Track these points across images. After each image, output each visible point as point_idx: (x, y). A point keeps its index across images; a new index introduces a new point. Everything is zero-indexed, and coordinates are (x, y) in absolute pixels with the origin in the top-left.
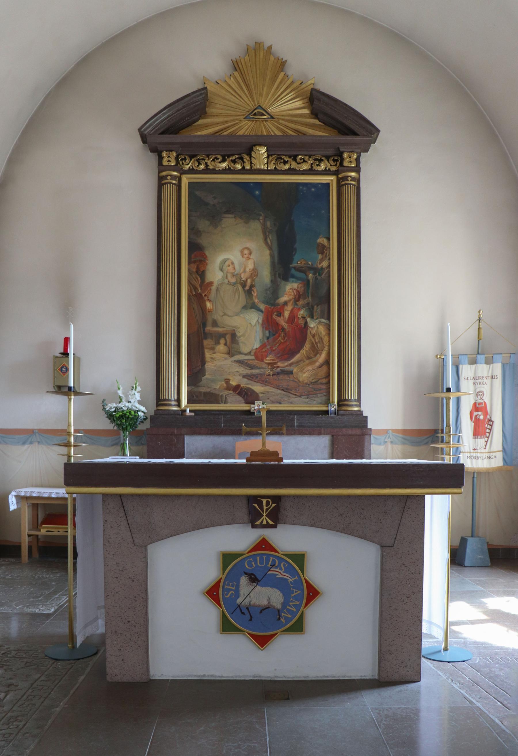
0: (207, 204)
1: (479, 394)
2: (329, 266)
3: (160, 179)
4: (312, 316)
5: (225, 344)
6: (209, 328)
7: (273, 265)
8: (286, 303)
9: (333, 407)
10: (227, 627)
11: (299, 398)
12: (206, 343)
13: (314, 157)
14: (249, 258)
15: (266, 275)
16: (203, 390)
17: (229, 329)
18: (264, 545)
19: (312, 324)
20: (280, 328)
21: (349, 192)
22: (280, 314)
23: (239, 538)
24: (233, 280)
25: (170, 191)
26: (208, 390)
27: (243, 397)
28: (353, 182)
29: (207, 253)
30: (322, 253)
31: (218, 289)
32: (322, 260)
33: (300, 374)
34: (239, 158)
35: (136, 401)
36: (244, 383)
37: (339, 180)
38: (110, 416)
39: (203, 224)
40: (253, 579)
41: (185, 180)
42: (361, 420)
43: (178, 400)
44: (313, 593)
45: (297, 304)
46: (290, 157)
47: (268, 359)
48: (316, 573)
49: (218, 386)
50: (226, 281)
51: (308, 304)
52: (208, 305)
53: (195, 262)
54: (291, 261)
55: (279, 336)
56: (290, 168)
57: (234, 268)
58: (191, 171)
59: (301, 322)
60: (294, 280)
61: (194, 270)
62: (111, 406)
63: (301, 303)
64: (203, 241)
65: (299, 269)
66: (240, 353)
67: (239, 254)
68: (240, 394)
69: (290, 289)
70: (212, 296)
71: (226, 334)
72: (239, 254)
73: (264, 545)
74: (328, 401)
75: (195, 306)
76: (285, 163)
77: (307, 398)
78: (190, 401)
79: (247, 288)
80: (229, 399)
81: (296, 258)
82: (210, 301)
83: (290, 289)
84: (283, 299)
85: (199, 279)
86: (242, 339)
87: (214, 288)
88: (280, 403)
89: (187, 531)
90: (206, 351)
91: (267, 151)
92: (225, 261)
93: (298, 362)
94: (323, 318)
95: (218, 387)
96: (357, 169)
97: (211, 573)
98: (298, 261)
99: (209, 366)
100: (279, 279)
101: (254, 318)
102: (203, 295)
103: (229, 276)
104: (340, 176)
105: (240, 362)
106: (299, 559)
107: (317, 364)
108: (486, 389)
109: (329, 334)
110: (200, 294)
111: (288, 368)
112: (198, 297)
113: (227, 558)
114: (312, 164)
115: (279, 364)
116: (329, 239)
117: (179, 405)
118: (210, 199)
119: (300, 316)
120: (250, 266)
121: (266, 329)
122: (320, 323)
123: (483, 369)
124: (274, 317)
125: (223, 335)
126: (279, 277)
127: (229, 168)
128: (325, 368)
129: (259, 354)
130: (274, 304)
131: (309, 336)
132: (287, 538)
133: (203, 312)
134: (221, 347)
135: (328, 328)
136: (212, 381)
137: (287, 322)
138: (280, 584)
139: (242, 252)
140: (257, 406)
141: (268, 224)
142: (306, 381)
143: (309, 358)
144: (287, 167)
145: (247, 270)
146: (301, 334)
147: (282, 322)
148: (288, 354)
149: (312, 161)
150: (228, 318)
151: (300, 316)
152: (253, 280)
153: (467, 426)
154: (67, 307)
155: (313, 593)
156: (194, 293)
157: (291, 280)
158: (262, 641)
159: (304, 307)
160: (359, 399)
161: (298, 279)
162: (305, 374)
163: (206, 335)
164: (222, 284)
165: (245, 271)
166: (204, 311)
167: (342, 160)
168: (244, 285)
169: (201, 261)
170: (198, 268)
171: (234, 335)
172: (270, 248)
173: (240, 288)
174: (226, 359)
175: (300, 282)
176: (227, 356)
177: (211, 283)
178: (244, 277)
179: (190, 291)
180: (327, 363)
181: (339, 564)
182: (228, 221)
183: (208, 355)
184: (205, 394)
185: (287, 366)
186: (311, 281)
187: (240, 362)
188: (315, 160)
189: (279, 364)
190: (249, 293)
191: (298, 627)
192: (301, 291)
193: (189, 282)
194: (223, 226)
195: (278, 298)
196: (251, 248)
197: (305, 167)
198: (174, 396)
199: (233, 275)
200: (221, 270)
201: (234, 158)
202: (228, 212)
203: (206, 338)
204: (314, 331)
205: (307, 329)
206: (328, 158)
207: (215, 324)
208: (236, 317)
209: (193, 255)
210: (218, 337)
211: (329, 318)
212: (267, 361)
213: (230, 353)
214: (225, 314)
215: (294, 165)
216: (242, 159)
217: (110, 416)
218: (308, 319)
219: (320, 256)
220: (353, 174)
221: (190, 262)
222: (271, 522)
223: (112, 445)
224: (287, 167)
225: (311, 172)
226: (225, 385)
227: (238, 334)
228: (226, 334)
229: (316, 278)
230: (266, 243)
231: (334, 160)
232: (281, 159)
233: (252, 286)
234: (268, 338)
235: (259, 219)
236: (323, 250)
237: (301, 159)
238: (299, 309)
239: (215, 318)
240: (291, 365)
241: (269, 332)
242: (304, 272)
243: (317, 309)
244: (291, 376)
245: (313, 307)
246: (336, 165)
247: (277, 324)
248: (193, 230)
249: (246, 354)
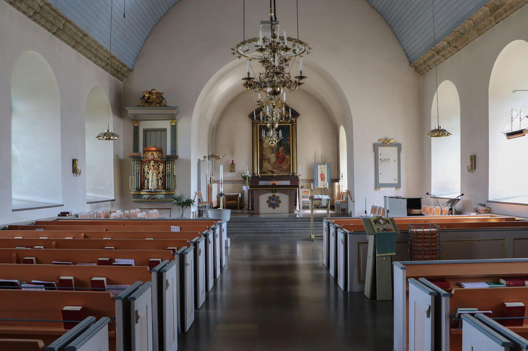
1: (322, 171)
9: (291, 175)
10: (269, 206)
12: (263, 161)
18: (274, 195)
21: (294, 127)
23: (271, 195)
25: (255, 128)
35: (248, 174)
36: (272, 169)
38: (243, 177)
41: (258, 125)
44: (280, 202)
48: (281, 199)
49: (266, 170)
62: (243, 175)
69: (281, 149)
73: (274, 195)
74: (290, 173)
83: (281, 149)
96: (296, 122)
97: (267, 199)
99: (264, 166)
101: (274, 155)
106: (278, 197)
108: (323, 170)
112: (261, 151)
113: (269, 197)
123: (323, 166)
129: (275, 163)
132: (277, 194)
135: (290, 157)
140: (275, 175)
146: (284, 158)
147: (280, 156)
148: (281, 163)
153: (319, 178)
154: (232, 153)
155: (280, 202)
158: (274, 208)
162: (285, 167)
166: (263, 153)
180: (290, 165)
181: (284, 198)
190: (272, 149)
191: (278, 206)
210: (266, 159)
213: (269, 163)
217: (243, 177)
236: (289, 140)
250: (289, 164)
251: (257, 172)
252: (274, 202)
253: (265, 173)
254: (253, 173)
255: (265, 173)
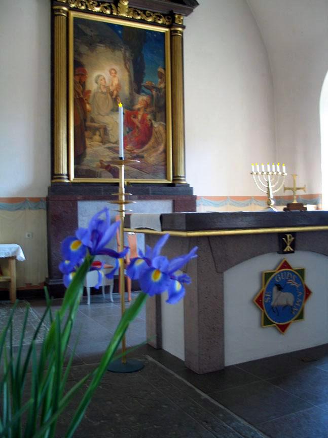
0: (86, 35)
2: (165, 88)
3: (53, 11)
4: (155, 120)
5: (100, 136)
6: (88, 123)
7: (131, 82)
8: (139, 109)
11: (148, 175)
12: (87, 134)
13: (157, 14)
14: (115, 76)
15: (126, 89)
16: (85, 168)
17: (102, 124)
19: (155, 125)
20: (136, 126)
22: (135, 117)
23: (269, 262)
24: (104, 90)
26: (88, 168)
27: (112, 173)
28: (180, 34)
29: (87, 70)
30: (161, 78)
31: (94, 96)
32: (161, 83)
33: (148, 158)
34: (109, 6)
37: (171, 31)
39: (84, 49)
40: (280, 288)
42: (188, 190)
43: (68, 175)
45: (146, 111)
46: (141, 10)
47: (128, 147)
50: (100, 91)
51: (153, 111)
52: (88, 106)
53: (78, 75)
54: (141, 81)
55: (135, 132)
56: (141, 19)
57: (105, 82)
58: (76, 9)
59: (149, 123)
60: (144, 94)
61: (78, 81)
63: (148, 110)
64: (84, 60)
65: (147, 87)
66: (110, 142)
67: (108, 74)
68: (110, 171)
69: (142, 99)
70: (90, 100)
71: (100, 128)
72: (108, 73)
73: (286, 265)
75: (79, 107)
76: (139, 15)
77: (153, 175)
78: (75, 176)
79: (114, 97)
80: (103, 175)
81: (145, 79)
82: (89, 104)
83: (141, 99)
84: (138, 106)
85: (81, 87)
86: (111, 132)
87: (91, 95)
88: (136, 178)
89: (246, 259)
90: (86, 139)
91: (129, 4)
92: (99, 76)
93: (147, 150)
94: (162, 121)
95: (95, 166)
97: (253, 287)
98: (146, 82)
99: (89, 151)
100: (134, 92)
102: (84, 99)
103: (102, 87)
104: (172, 29)
105: (109, 148)
107: (159, 152)
109: (166, 132)
110: (82, 98)
111: (141, 154)
114: (155, 18)
115: (135, 151)
116: (165, 69)
117: (69, 179)
118: (88, 31)
119: (148, 119)
120: (116, 82)
121: (127, 126)
122: (160, 124)
124: (132, 118)
125: (97, 129)
126: (135, 91)
127: (102, 12)
128: (163, 154)
130: (131, 110)
131: (154, 132)
132: (297, 260)
133: (84, 112)
134: (97, 137)
136: (91, 162)
137: (140, 123)
138: (292, 290)
139: (110, 72)
141: (128, 54)
142: (152, 163)
143: (154, 148)
144: (139, 18)
145: (114, 84)
146: (148, 132)
148: (141, 144)
149: (155, 17)
150: (102, 117)
151: (148, 119)
152: (118, 92)
156: (78, 97)
157: (142, 94)
158: (283, 328)
159: (150, 113)
160: (185, 177)
161: (147, 94)
162: (153, 158)
163: (87, 128)
164: (97, 93)
165: (112, 85)
166: (85, 111)
167: (174, 19)
168: (112, 94)
169: (82, 75)
170: (80, 80)
171: (105, 129)
172: (129, 71)
173: (109, 97)
174: (100, 146)
175: (148, 96)
176: (101, 144)
177: (89, 92)
178: (112, 89)
179: (75, 96)
180: (165, 151)
182: (101, 48)
183: (88, 142)
184: (87, 171)
185: (140, 152)
186: (154, 96)
187: (109, 148)
188: (156, 16)
189: (135, 151)
192: (149, 102)
193: (75, 90)
194: (98, 52)
195: (133, 105)
196: (117, 70)
197: (150, 20)
198: (65, 172)
199: (105, 87)
200: (97, 82)
201: (105, 5)
202: (101, 42)
203: (86, 130)
204: (157, 130)
205: (152, 128)
206: (164, 15)
207: (93, 120)
208: (107, 117)
209: (77, 70)
211: (165, 121)
212: (127, 149)
213: (103, 142)
214: (99, 114)
215: (144, 17)
216: (111, 7)
218: (153, 122)
219: (160, 80)
220: (180, 29)
221: (75, 75)
222: (292, 250)
223: (16, 210)
224: (139, 18)
225: (154, 23)
226: (100, 164)
227: (108, 129)
228: (100, 128)
229: (158, 95)
230: (126, 68)
231: (168, 18)
232: (136, 11)
233: (117, 96)
234: (128, 132)
235: (121, 50)
236: (162, 76)
237: (148, 14)
238: (147, 114)
239: (93, 117)
240: (143, 152)
241: (129, 128)
242: (150, 90)
243: (159, 115)
244: (143, 159)
245: (155, 113)
246: (169, 21)
247: (134, 124)
248: (76, 51)
249: (113, 143)
250: (161, 148)
251: (68, 168)
252: (283, 299)
253: (91, 174)
254: (54, 174)
255: (91, 174)
